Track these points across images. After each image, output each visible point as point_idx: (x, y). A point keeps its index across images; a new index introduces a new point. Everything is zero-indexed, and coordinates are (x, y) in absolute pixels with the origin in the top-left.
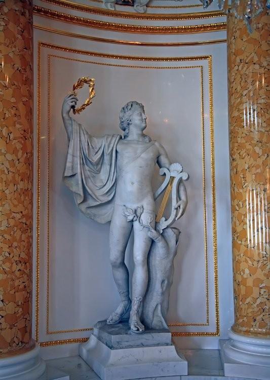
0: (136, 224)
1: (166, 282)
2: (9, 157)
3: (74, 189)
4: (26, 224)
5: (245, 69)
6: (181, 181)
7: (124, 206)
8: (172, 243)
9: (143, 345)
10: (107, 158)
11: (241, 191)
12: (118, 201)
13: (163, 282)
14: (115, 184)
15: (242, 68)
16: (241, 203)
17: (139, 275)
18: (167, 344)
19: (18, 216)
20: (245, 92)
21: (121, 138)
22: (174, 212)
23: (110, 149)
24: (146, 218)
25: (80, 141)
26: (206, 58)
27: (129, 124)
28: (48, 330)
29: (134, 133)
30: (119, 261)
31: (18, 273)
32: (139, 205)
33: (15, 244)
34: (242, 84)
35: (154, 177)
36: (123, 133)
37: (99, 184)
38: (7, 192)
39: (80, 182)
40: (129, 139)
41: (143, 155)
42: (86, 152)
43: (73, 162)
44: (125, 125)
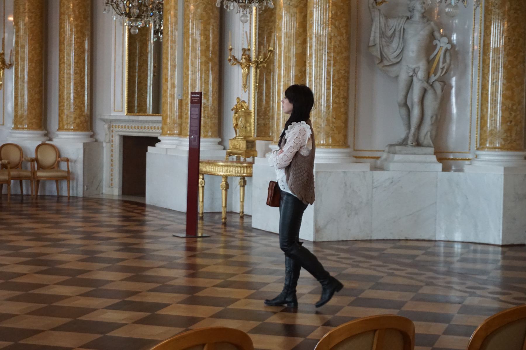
0: (415, 79)
1: (434, 117)
2: (339, 38)
3: (375, 54)
6: (447, 50)
9: (415, 154)
10: (397, 33)
12: (404, 63)
13: (432, 117)
17: (416, 112)
18: (431, 154)
19: (343, 72)
21: (408, 18)
22: (440, 71)
23: (399, 28)
24: (421, 74)
25: (380, 22)
29: (417, 16)
30: (403, 102)
31: (342, 105)
33: (341, 88)
35: (429, 48)
36: (409, 14)
37: (392, 51)
38: (338, 58)
39: (379, 50)
40: (413, 19)
41: (422, 33)
42: (384, 30)
43: (375, 35)
44: (411, 10)
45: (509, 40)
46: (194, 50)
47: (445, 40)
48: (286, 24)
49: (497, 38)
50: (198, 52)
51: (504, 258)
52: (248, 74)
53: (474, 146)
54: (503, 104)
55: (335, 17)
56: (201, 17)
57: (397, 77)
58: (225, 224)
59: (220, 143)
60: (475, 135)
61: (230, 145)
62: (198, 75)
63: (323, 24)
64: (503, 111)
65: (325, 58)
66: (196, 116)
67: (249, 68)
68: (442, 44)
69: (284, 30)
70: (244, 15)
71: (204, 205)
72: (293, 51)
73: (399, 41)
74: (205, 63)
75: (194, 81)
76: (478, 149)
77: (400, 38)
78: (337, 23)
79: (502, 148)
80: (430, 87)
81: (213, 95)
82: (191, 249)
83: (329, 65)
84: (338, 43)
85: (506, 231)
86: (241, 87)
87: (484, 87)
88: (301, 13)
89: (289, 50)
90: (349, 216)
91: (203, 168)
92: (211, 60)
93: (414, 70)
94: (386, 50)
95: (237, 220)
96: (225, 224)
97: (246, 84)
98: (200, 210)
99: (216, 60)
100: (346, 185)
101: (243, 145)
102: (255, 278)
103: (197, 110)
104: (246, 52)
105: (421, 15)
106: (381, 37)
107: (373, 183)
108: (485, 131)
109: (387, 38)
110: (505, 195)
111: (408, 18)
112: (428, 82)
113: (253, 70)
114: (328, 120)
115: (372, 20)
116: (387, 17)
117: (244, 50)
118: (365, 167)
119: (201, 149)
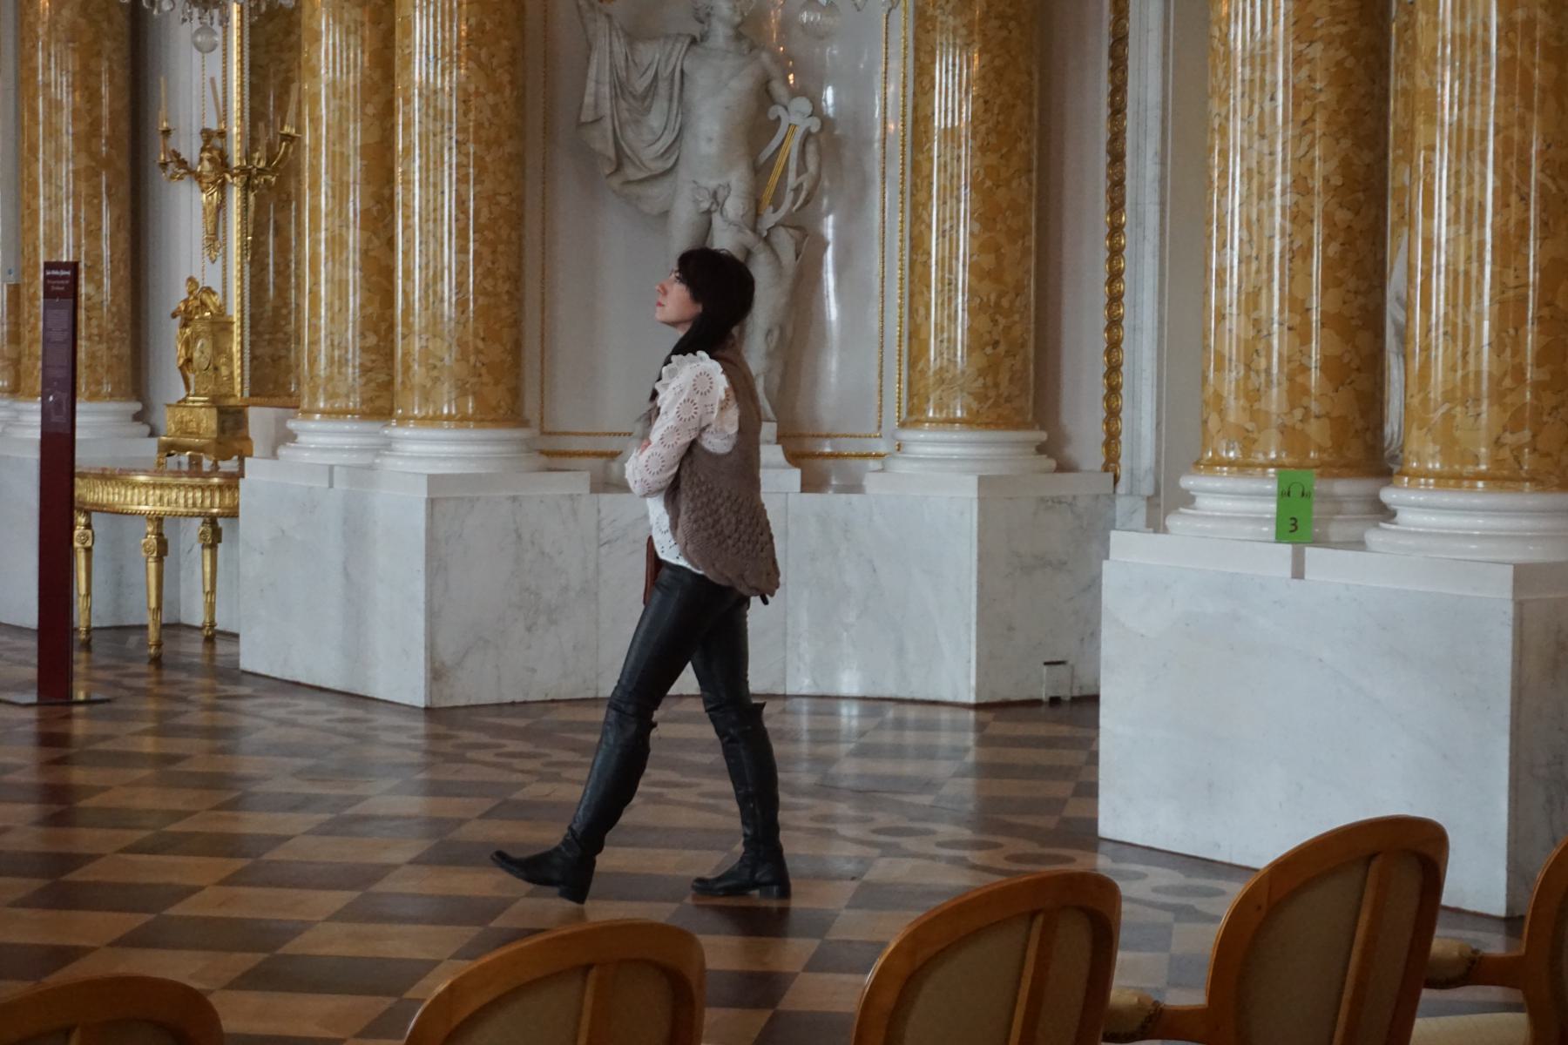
0: (717, 219)
1: (776, 333)
2: (490, 98)
3: (598, 146)
6: (807, 135)
8: (788, 256)
10: (663, 87)
12: (683, 173)
13: (769, 332)
14: (679, 138)
19: (504, 200)
21: (694, 41)
22: (789, 197)
23: (670, 69)
24: (734, 206)
25: (611, 52)
29: (720, 34)
31: (506, 298)
32: (722, 181)
33: (501, 248)
35: (757, 126)
36: (695, 29)
37: (649, 137)
38: (488, 159)
39: (610, 134)
40: (709, 44)
41: (735, 84)
42: (623, 74)
43: (597, 88)
44: (702, 15)
45: (985, 103)
46: (53, 133)
47: (803, 105)
48: (331, 55)
49: (953, 99)
50: (67, 141)
51: (984, 741)
52: (221, 206)
53: (892, 416)
54: (972, 292)
55: (476, 37)
56: (73, 35)
57: (665, 214)
58: (157, 661)
59: (139, 417)
60: (895, 388)
61: (168, 422)
62: (67, 210)
63: (443, 57)
64: (972, 312)
65: (451, 158)
66: (61, 336)
67: (223, 188)
68: (795, 117)
69: (325, 74)
70: (206, 29)
71: (92, 605)
72: (355, 137)
73: (670, 108)
74: (86, 175)
75: (55, 227)
76: (903, 425)
77: (671, 100)
78: (484, 53)
79: (971, 422)
80: (761, 245)
81: (114, 272)
82: (52, 740)
83: (462, 180)
84: (488, 113)
85: (987, 663)
86: (201, 248)
87: (917, 244)
88: (376, 22)
89: (343, 136)
90: (529, 629)
91: (85, 492)
92: (108, 163)
93: (715, 195)
94: (630, 134)
95: (194, 648)
96: (157, 661)
97: (215, 239)
98: (80, 620)
99: (123, 164)
100: (519, 537)
101: (208, 421)
102: (253, 823)
103: (65, 314)
104: (213, 139)
105: (730, 32)
106: (615, 97)
107: (599, 528)
108: (923, 373)
109: (633, 98)
110: (981, 558)
111: (694, 41)
112: (754, 230)
113: (235, 195)
114: (462, 345)
115: (590, 47)
116: (634, 36)
117: (207, 135)
118: (575, 482)
119: (79, 435)
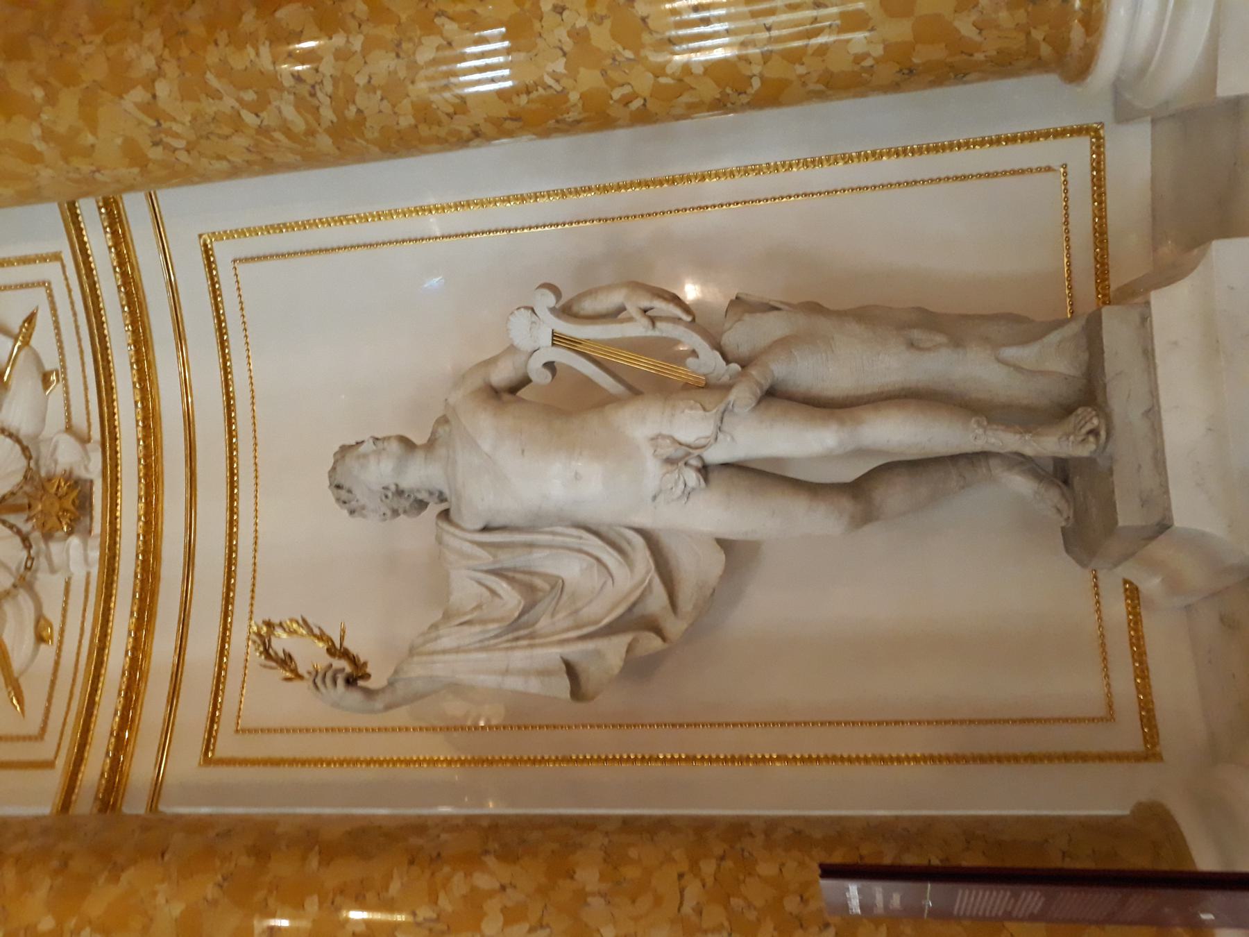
0: (715, 455)
1: (916, 334)
4: (722, 858)
5: (176, 128)
7: (655, 498)
10: (506, 559)
11: (574, 97)
12: (644, 519)
13: (912, 345)
15: (177, 136)
16: (617, 94)
18: (1145, 319)
20: (249, 118)
24: (690, 425)
26: (207, 252)
27: (400, 493)
28: (1102, 719)
29: (420, 474)
30: (846, 503)
32: (647, 451)
34: (226, 130)
39: (590, 645)
41: (486, 446)
44: (405, 503)
57: (725, 544)
73: (550, 546)
77: (531, 546)
80: (754, 372)
111: (445, 515)
112: (727, 388)
